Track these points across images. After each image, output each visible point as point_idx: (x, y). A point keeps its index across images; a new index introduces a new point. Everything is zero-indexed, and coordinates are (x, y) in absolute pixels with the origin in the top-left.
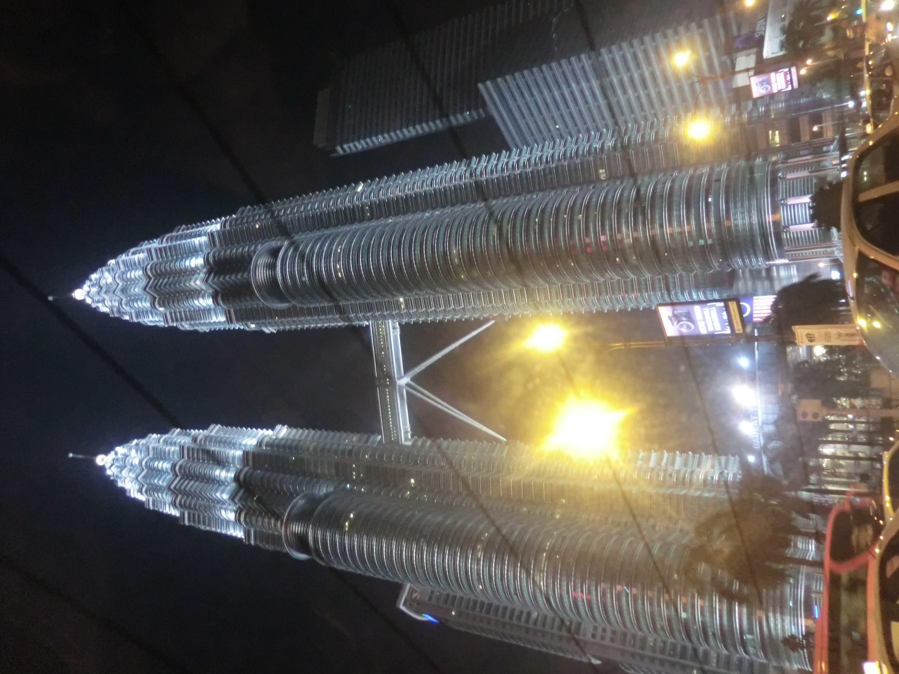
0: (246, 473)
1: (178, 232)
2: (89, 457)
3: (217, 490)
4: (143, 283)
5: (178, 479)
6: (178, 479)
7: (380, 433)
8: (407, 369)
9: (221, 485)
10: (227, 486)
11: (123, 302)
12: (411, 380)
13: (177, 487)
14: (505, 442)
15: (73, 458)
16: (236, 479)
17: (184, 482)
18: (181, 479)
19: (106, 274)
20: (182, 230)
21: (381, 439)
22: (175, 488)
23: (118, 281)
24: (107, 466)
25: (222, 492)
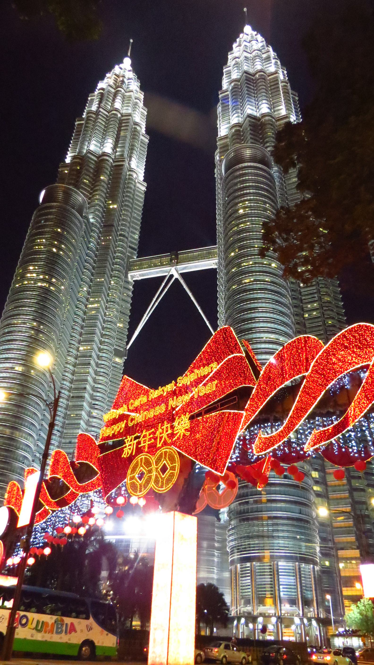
0: (107, 160)
1: (292, 94)
2: (129, 54)
3: (97, 141)
4: (251, 71)
5: (107, 113)
6: (107, 113)
7: (137, 257)
8: (183, 275)
9: (101, 144)
10: (100, 148)
11: (237, 59)
12: (177, 279)
13: (100, 113)
14: (126, 348)
15: (130, 42)
16: (104, 154)
17: (105, 118)
18: (107, 116)
19: (260, 45)
20: (294, 96)
21: (134, 258)
22: (100, 111)
23: (254, 54)
24: (121, 65)
25: (96, 146)
